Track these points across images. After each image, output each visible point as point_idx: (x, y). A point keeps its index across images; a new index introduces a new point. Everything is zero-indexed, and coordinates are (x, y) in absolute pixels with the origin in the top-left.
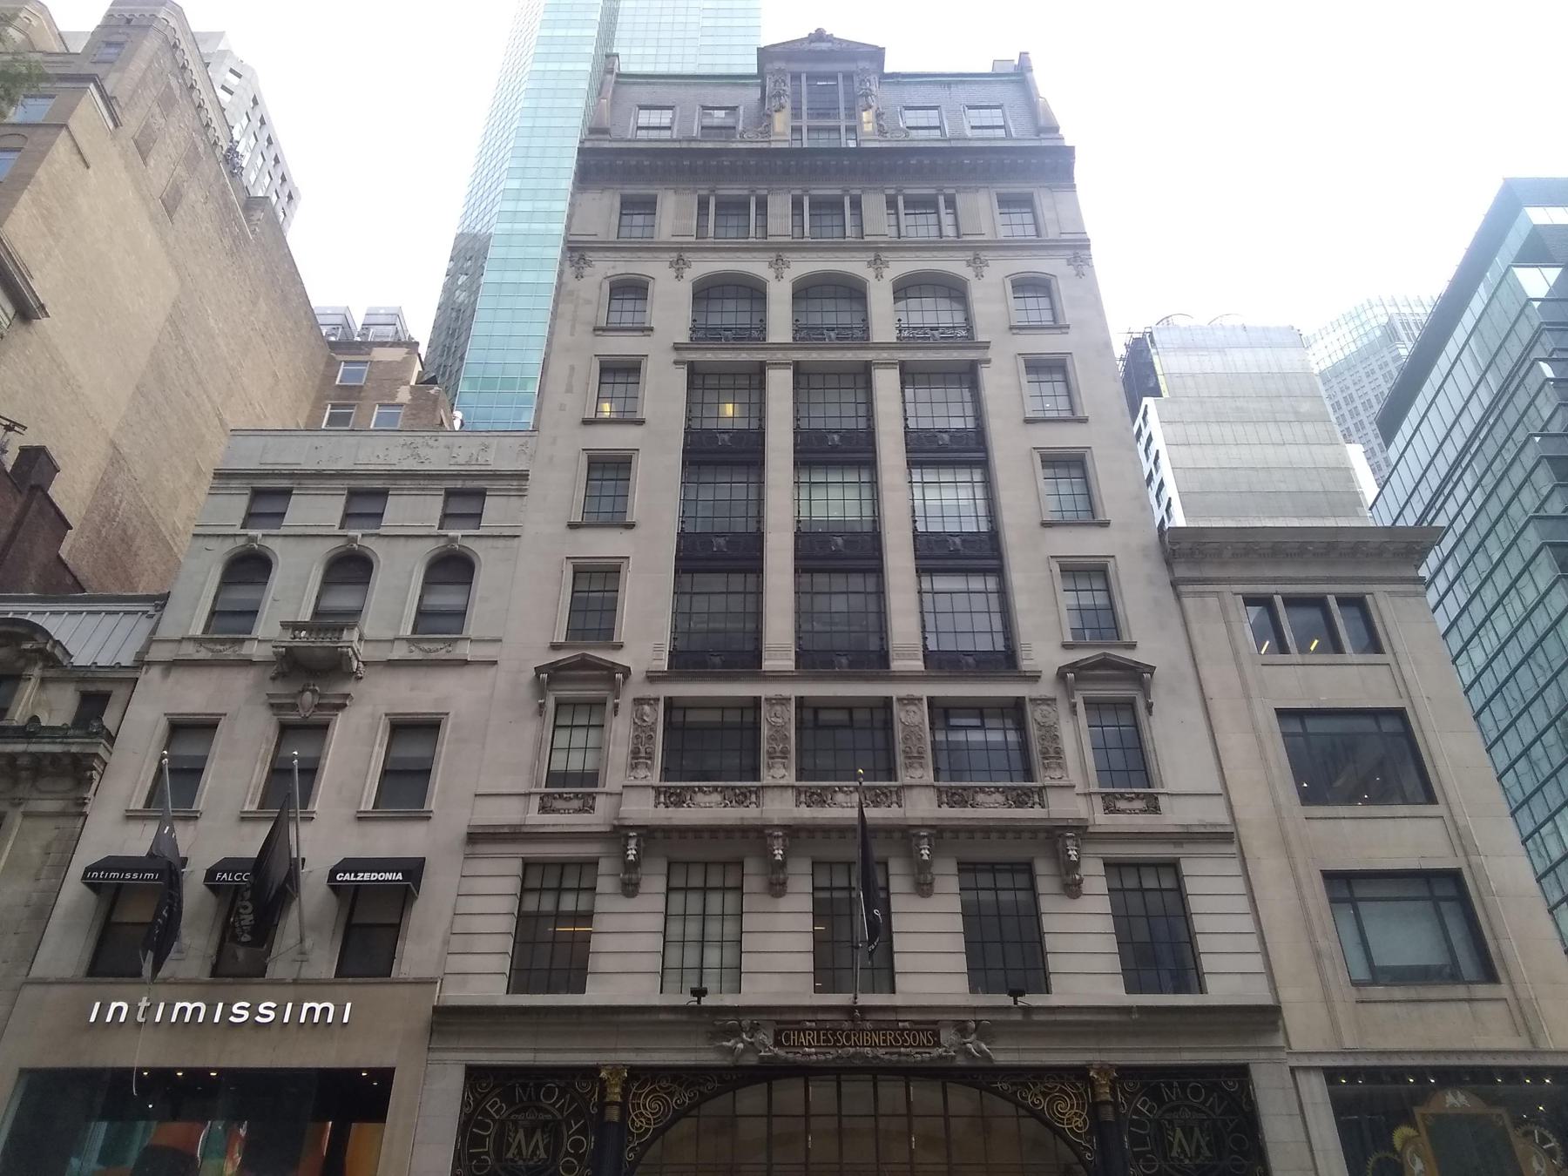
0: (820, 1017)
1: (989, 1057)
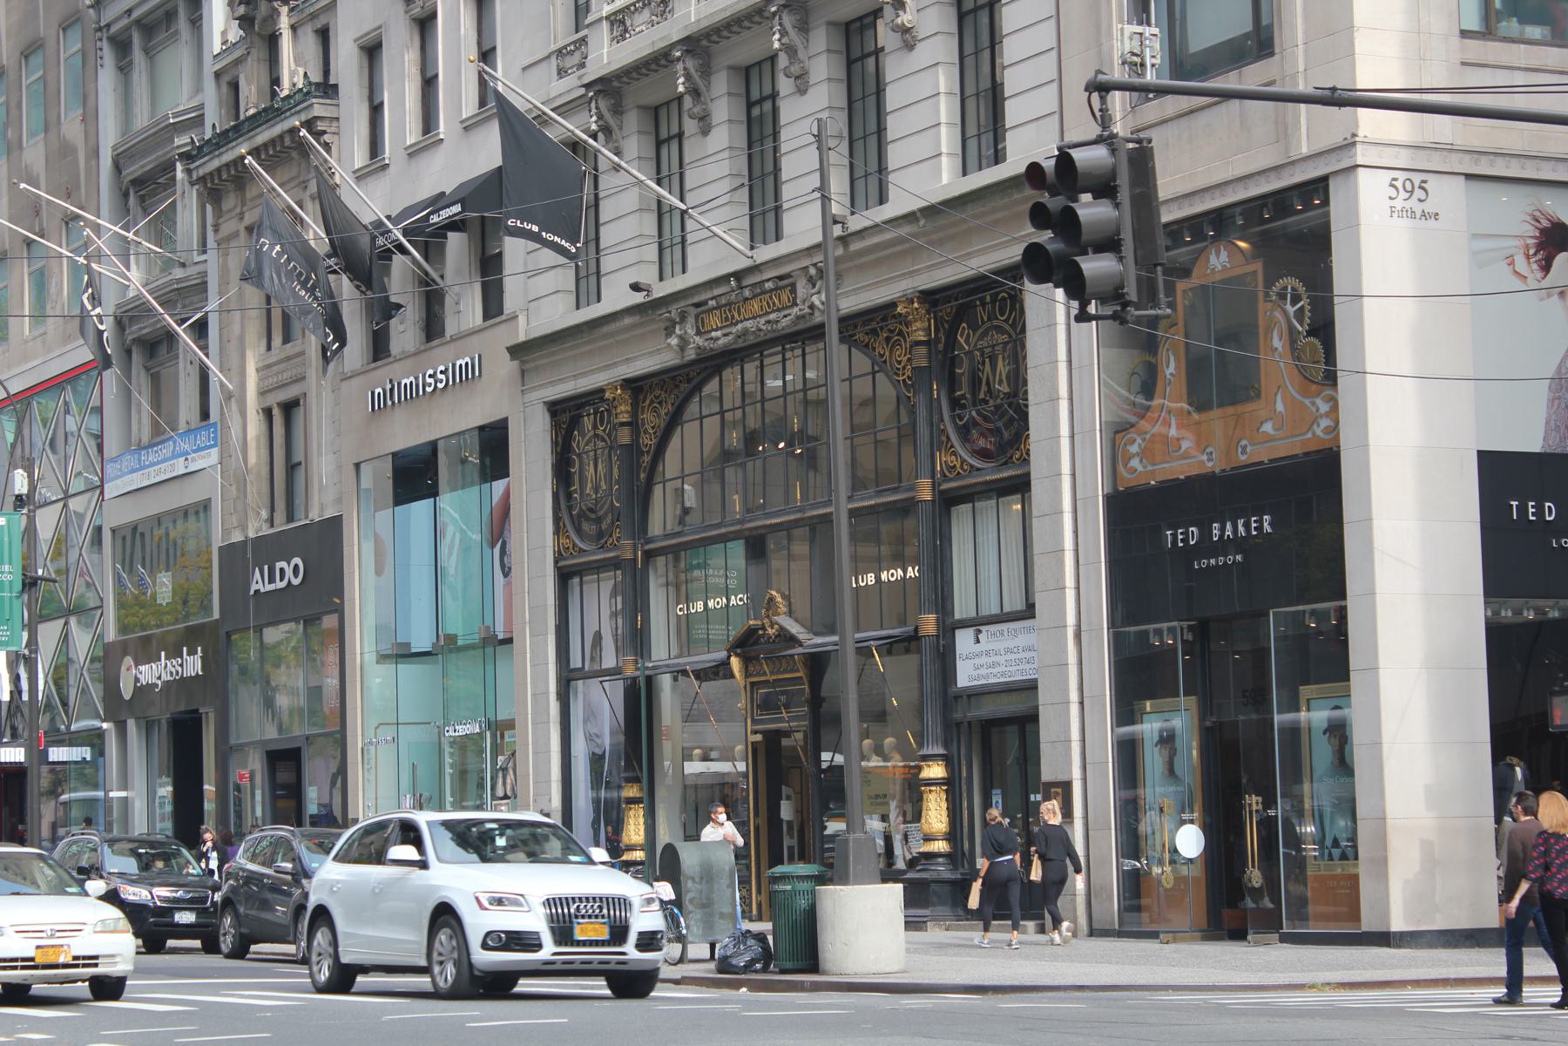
0: (717, 292)
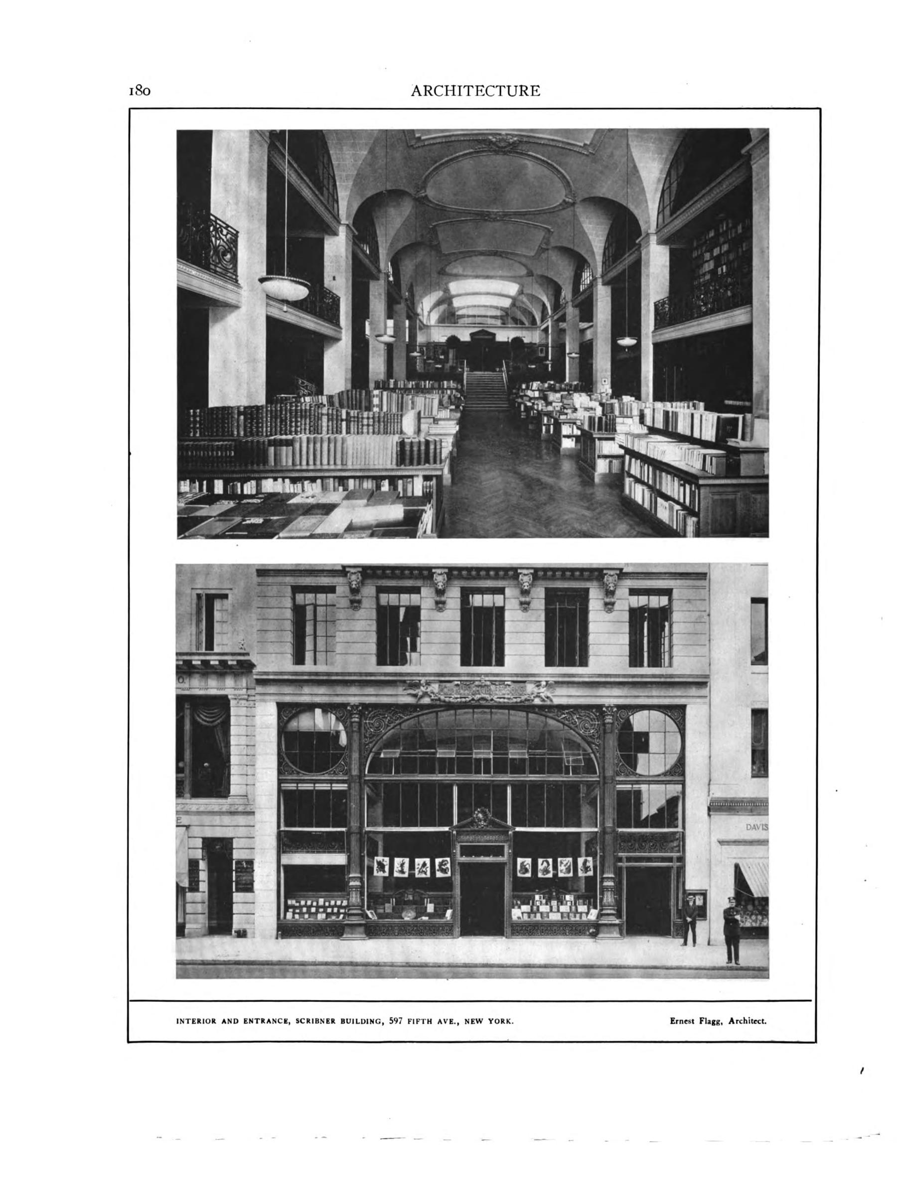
0: (463, 678)
1: (551, 701)
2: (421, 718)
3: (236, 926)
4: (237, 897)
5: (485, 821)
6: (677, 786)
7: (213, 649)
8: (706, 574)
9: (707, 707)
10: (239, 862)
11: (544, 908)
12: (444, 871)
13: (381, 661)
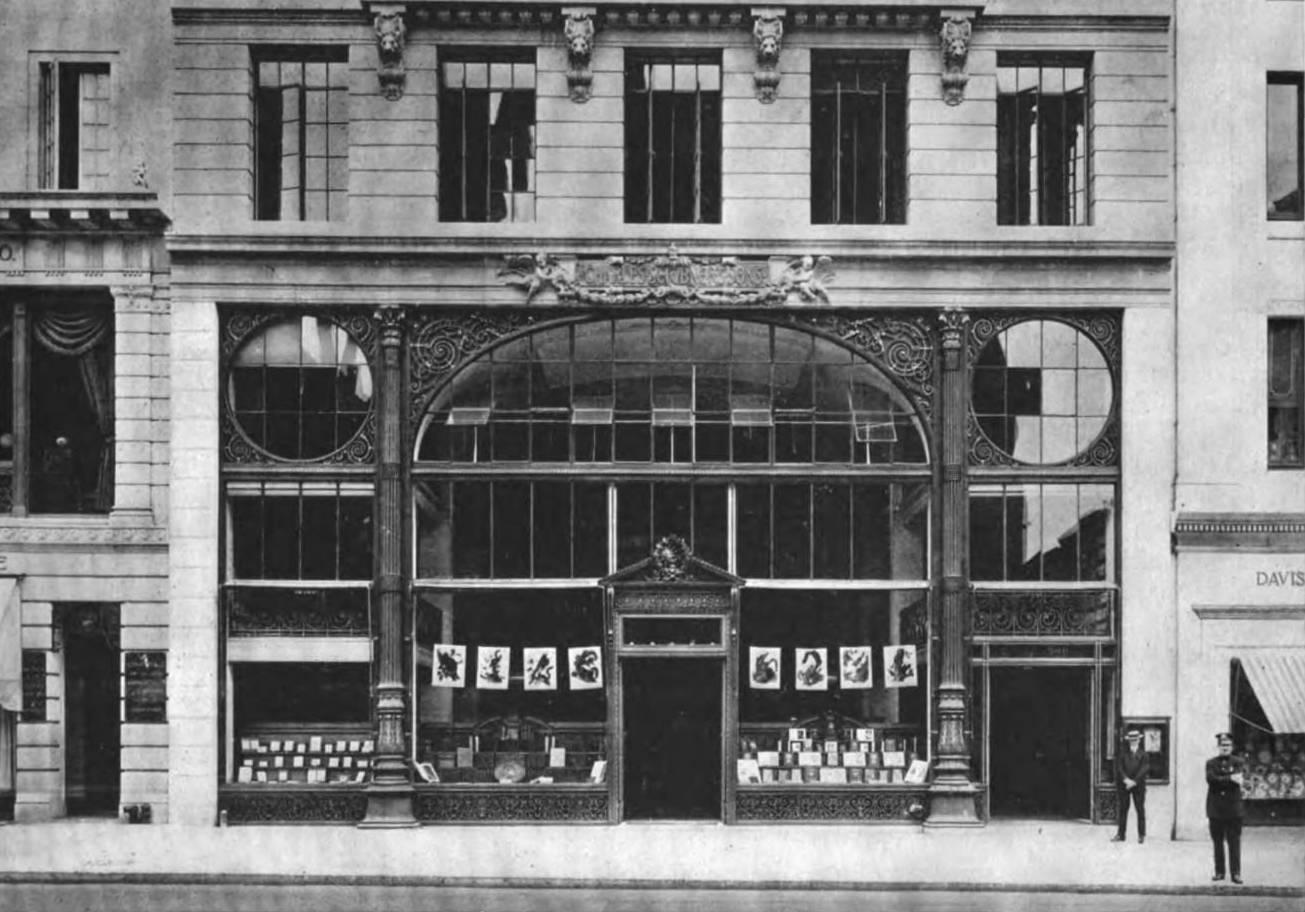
0: (630, 250)
1: (825, 299)
2: (537, 338)
3: (126, 798)
4: (130, 733)
5: (678, 565)
6: (1102, 488)
7: (75, 186)
8: (1166, 19)
9: (1169, 313)
10: (133, 656)
11: (809, 759)
12: (588, 676)
13: (448, 213)
